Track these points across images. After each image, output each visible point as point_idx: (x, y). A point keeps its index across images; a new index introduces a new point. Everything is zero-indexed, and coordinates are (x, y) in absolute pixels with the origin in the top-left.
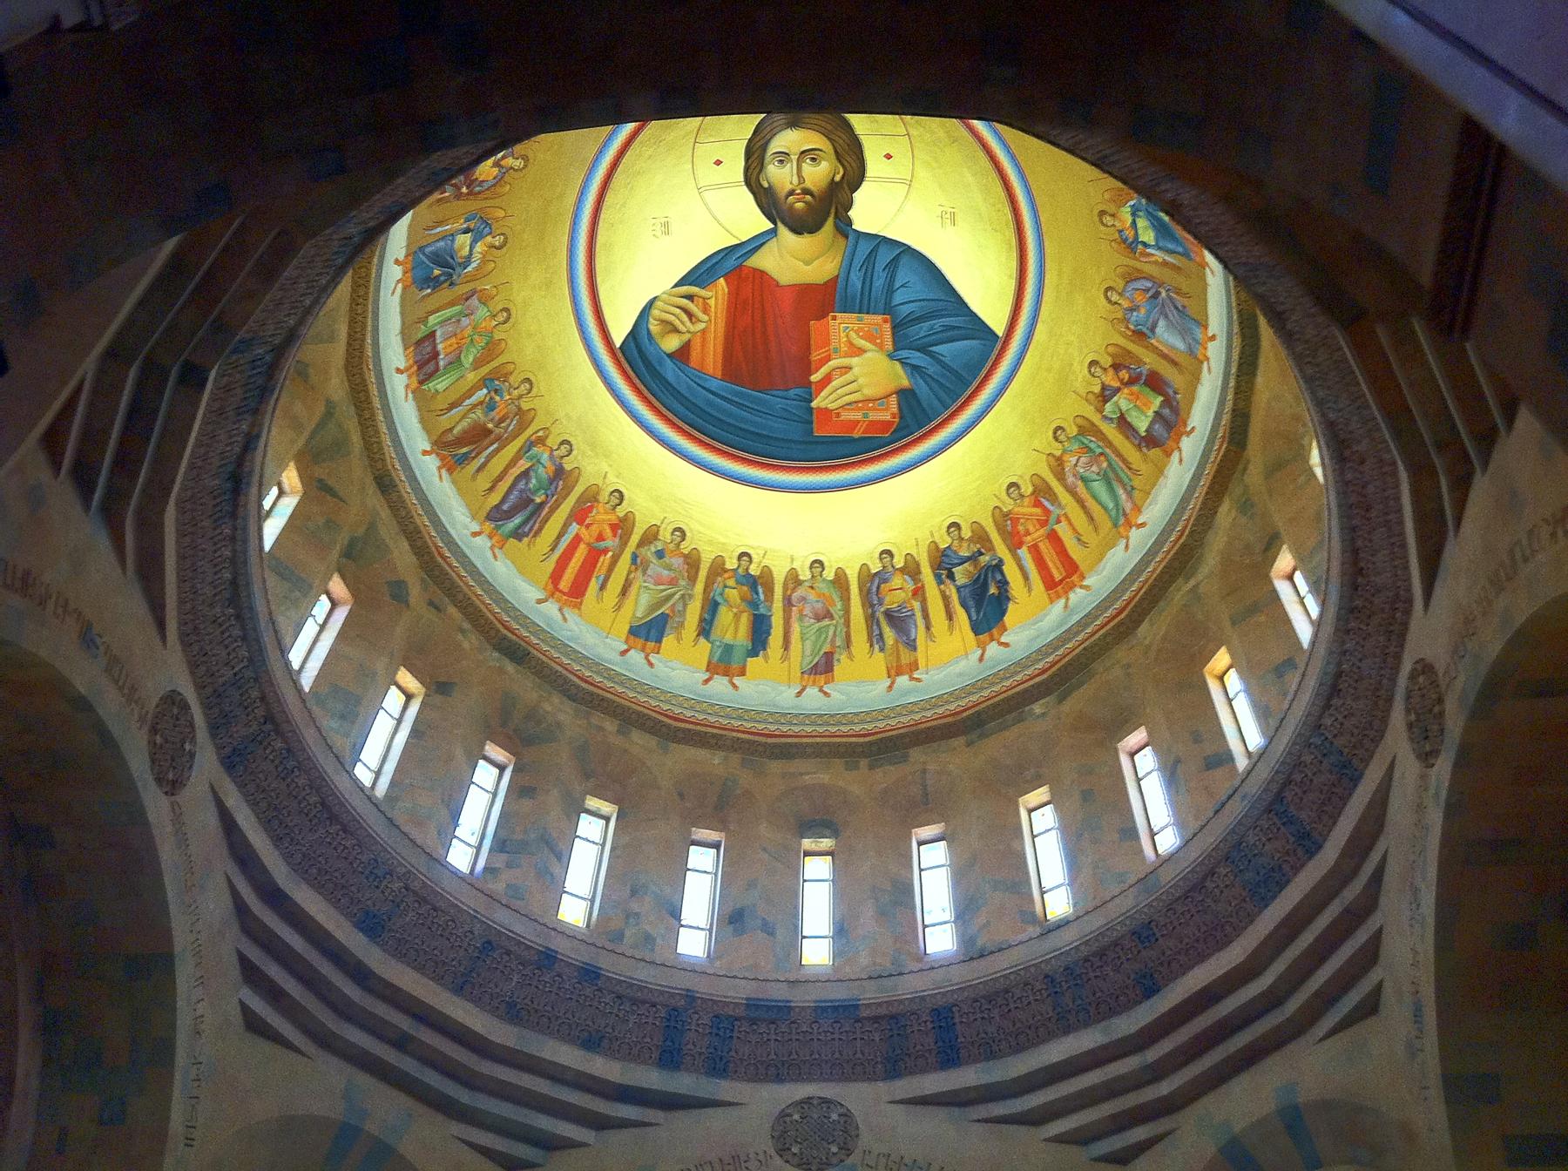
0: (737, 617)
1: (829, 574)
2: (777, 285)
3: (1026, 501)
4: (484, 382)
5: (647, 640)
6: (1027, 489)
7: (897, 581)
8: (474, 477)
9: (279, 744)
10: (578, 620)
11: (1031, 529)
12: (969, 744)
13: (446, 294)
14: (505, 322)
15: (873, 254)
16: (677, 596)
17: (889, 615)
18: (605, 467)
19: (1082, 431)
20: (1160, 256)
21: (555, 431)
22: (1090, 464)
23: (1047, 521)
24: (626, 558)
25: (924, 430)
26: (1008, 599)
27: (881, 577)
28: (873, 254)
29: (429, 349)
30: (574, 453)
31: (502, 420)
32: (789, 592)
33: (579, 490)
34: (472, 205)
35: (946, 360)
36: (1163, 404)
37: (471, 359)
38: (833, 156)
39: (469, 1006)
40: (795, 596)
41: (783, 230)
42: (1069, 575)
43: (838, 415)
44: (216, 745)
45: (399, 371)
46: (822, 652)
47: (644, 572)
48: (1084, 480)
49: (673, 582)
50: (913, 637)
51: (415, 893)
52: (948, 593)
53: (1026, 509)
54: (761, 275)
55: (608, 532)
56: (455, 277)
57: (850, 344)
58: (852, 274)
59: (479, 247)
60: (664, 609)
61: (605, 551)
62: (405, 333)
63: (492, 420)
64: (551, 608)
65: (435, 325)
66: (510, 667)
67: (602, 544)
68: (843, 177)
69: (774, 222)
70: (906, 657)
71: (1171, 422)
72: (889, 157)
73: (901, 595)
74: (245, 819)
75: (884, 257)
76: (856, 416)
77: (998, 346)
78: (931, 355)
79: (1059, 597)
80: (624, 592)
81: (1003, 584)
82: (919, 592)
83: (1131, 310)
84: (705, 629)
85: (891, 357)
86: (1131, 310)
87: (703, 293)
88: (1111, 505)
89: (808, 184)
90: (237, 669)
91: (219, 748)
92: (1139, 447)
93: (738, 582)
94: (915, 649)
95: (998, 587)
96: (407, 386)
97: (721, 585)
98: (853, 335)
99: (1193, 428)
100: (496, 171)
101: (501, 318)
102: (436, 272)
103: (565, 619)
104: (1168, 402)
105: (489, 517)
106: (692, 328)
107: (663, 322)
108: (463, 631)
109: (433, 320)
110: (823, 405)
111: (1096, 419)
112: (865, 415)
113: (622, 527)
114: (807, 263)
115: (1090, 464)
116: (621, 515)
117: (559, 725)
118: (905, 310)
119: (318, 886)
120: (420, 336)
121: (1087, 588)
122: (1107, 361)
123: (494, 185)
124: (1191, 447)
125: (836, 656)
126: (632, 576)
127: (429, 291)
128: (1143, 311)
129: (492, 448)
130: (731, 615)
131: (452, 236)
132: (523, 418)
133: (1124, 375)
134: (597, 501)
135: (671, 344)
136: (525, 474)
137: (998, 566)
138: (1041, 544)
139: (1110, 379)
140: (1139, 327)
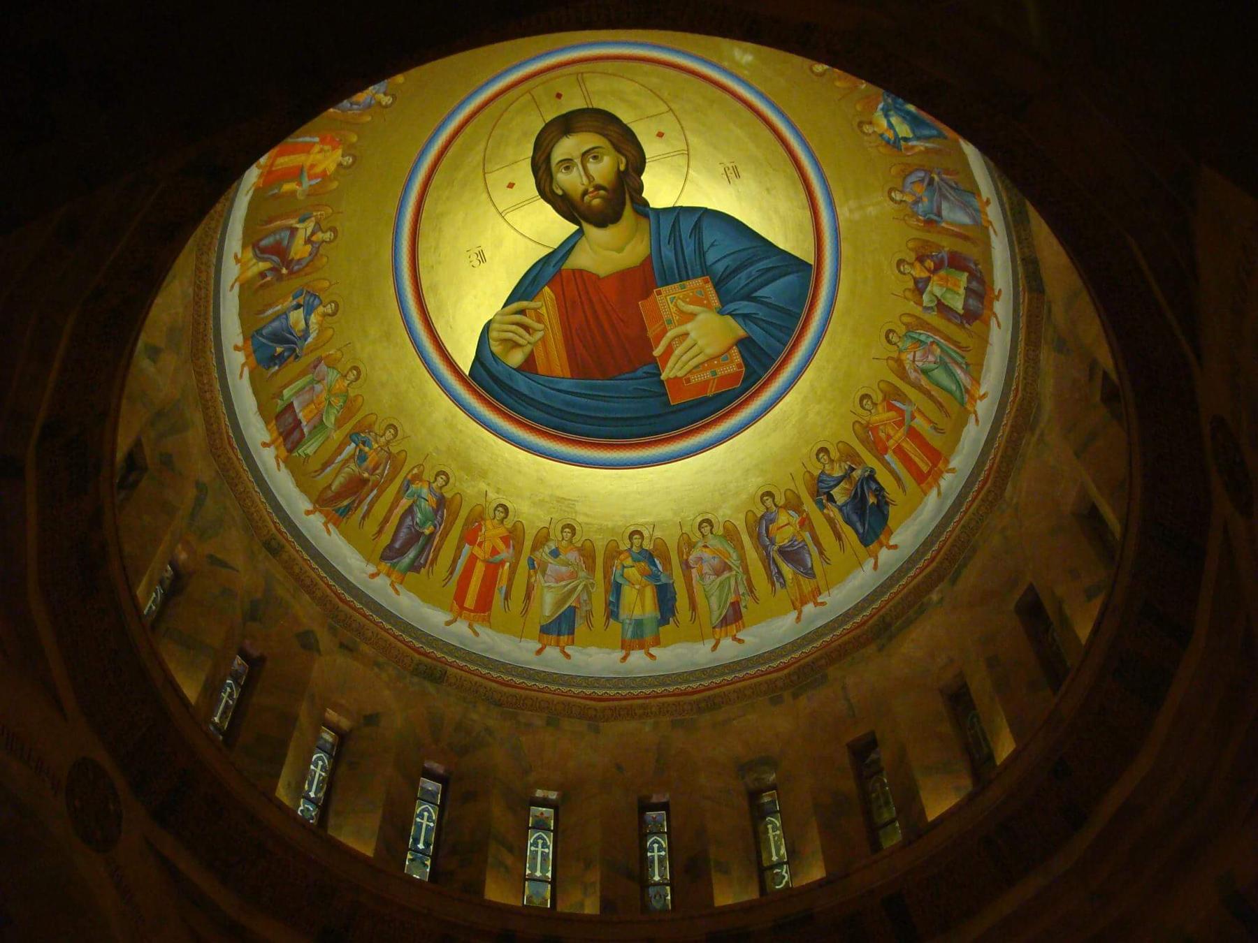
0: (641, 593)
2: (597, 277)
3: (880, 408)
4: (352, 437)
5: (559, 635)
6: (878, 397)
7: (783, 518)
8: (361, 524)
10: (489, 631)
11: (892, 433)
12: (881, 649)
13: (293, 367)
14: (357, 379)
16: (580, 588)
17: (783, 552)
18: (483, 486)
20: (920, 146)
22: (925, 356)
23: (904, 419)
24: (524, 563)
25: (771, 371)
26: (887, 503)
29: (290, 420)
30: (451, 481)
31: (376, 468)
32: (685, 557)
33: (464, 513)
34: (296, 283)
35: (772, 301)
36: (969, 281)
37: (333, 419)
40: (692, 559)
41: (586, 227)
42: (935, 465)
43: (688, 381)
45: (265, 445)
46: (728, 604)
47: (544, 573)
48: (925, 372)
49: (573, 576)
50: (810, 565)
52: (832, 515)
53: (881, 416)
54: (580, 273)
55: (501, 545)
57: (681, 312)
59: (314, 319)
60: (571, 602)
61: (502, 563)
62: (262, 409)
63: (366, 470)
64: (461, 627)
65: (291, 396)
66: (431, 688)
67: (498, 558)
68: (627, 165)
70: (807, 584)
71: (980, 291)
72: (660, 135)
73: (789, 531)
75: (686, 226)
76: (707, 375)
79: (931, 487)
80: (528, 596)
81: (880, 491)
82: (805, 523)
83: (916, 202)
84: (612, 611)
85: (721, 313)
86: (916, 202)
88: (954, 387)
89: (599, 180)
92: (961, 326)
94: (814, 576)
95: (877, 496)
96: (277, 457)
98: (680, 303)
99: (1000, 291)
100: (309, 247)
101: (351, 376)
102: (279, 350)
103: (477, 634)
104: (972, 276)
105: (384, 558)
106: (532, 339)
107: (504, 341)
109: (287, 393)
110: (672, 375)
111: (918, 311)
112: (714, 373)
113: (513, 537)
114: (620, 250)
116: (509, 526)
117: (488, 730)
118: (720, 267)
120: (279, 409)
121: (953, 470)
122: (911, 257)
123: (312, 261)
124: (1002, 308)
125: (743, 604)
126: (533, 580)
127: (277, 368)
128: (925, 200)
129: (372, 495)
130: (635, 592)
131: (285, 314)
132: (395, 461)
133: (930, 264)
134: (483, 519)
135: (516, 358)
136: (410, 511)
137: (871, 477)
138: (904, 445)
139: (918, 272)
140: (928, 216)
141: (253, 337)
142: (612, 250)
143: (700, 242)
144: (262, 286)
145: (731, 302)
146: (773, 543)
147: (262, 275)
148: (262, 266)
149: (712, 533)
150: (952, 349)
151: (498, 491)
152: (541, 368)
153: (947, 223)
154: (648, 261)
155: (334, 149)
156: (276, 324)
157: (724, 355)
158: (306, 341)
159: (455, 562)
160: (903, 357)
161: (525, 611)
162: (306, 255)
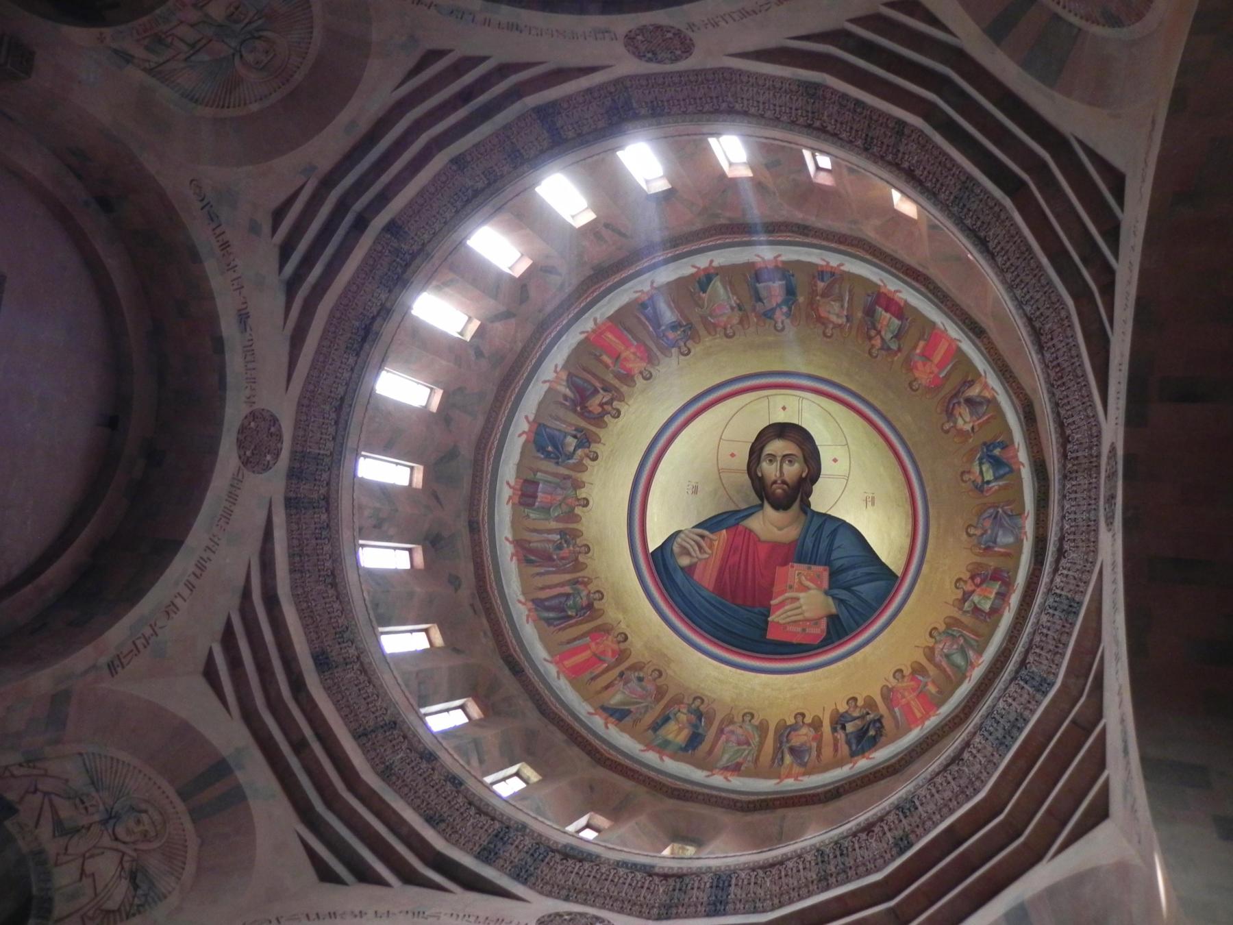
0: (681, 730)
1: (756, 722)
2: (759, 540)
3: (906, 679)
4: (562, 532)
6: (907, 671)
7: (804, 730)
9: (324, 517)
15: (821, 527)
17: (792, 750)
18: (621, 617)
19: (948, 626)
20: (995, 485)
21: (595, 582)
22: (952, 645)
24: (617, 671)
27: (794, 728)
28: (821, 527)
30: (603, 601)
33: (599, 622)
35: (863, 596)
37: (556, 514)
38: (802, 460)
39: (359, 751)
40: (727, 729)
44: (287, 485)
47: (626, 683)
50: (806, 760)
51: (362, 664)
53: (906, 683)
54: (749, 532)
56: (560, 460)
57: (800, 582)
58: (807, 539)
59: (580, 452)
60: (632, 708)
61: (603, 661)
66: (507, 671)
69: (762, 500)
73: (805, 738)
74: (280, 535)
76: (799, 629)
77: (899, 581)
78: (853, 592)
80: (607, 687)
82: (819, 738)
85: (826, 593)
87: (711, 536)
89: (787, 478)
90: (322, 452)
91: (288, 488)
93: (688, 711)
95: (876, 731)
96: (510, 498)
97: (676, 709)
98: (803, 578)
100: (600, 410)
102: (550, 448)
105: (533, 601)
106: (700, 556)
108: (485, 633)
110: (776, 620)
112: (804, 630)
113: (622, 655)
114: (780, 529)
115: (952, 645)
118: (838, 564)
119: (300, 611)
120: (529, 478)
122: (966, 576)
126: (616, 682)
127: (542, 456)
129: (551, 569)
130: (677, 727)
133: (978, 580)
135: (684, 561)
136: (568, 595)
137: (879, 720)
138: (913, 703)
139: (969, 587)
141: (540, 425)
142: (776, 526)
143: (831, 544)
144: (562, 404)
145: (839, 588)
146: (788, 741)
147: (566, 397)
148: (568, 392)
149: (750, 721)
150: (973, 639)
151: (628, 626)
152: (696, 577)
153: (1000, 547)
154: (793, 544)
155: (642, 359)
156: (557, 433)
157: (815, 622)
158: (569, 459)
159: (575, 639)
160: (937, 646)
161: (599, 692)
162: (596, 412)
